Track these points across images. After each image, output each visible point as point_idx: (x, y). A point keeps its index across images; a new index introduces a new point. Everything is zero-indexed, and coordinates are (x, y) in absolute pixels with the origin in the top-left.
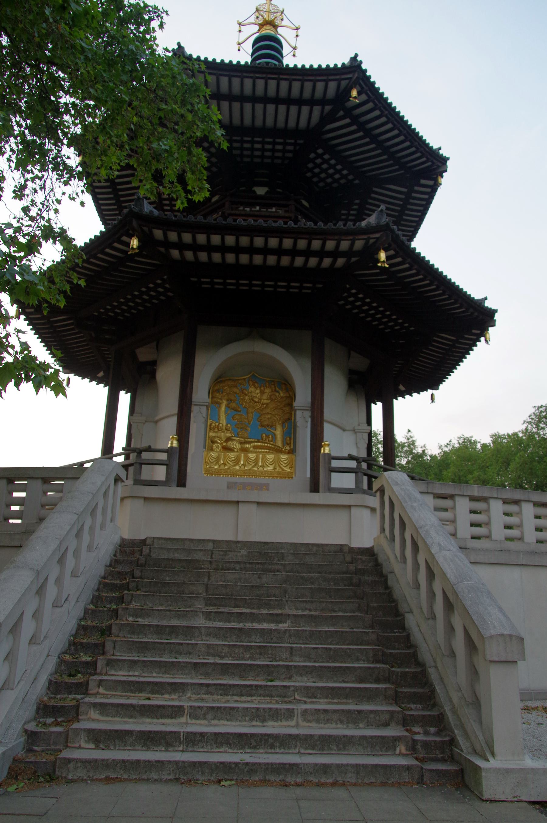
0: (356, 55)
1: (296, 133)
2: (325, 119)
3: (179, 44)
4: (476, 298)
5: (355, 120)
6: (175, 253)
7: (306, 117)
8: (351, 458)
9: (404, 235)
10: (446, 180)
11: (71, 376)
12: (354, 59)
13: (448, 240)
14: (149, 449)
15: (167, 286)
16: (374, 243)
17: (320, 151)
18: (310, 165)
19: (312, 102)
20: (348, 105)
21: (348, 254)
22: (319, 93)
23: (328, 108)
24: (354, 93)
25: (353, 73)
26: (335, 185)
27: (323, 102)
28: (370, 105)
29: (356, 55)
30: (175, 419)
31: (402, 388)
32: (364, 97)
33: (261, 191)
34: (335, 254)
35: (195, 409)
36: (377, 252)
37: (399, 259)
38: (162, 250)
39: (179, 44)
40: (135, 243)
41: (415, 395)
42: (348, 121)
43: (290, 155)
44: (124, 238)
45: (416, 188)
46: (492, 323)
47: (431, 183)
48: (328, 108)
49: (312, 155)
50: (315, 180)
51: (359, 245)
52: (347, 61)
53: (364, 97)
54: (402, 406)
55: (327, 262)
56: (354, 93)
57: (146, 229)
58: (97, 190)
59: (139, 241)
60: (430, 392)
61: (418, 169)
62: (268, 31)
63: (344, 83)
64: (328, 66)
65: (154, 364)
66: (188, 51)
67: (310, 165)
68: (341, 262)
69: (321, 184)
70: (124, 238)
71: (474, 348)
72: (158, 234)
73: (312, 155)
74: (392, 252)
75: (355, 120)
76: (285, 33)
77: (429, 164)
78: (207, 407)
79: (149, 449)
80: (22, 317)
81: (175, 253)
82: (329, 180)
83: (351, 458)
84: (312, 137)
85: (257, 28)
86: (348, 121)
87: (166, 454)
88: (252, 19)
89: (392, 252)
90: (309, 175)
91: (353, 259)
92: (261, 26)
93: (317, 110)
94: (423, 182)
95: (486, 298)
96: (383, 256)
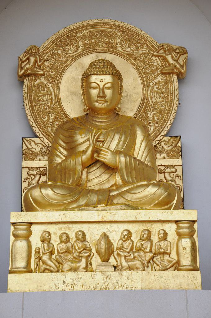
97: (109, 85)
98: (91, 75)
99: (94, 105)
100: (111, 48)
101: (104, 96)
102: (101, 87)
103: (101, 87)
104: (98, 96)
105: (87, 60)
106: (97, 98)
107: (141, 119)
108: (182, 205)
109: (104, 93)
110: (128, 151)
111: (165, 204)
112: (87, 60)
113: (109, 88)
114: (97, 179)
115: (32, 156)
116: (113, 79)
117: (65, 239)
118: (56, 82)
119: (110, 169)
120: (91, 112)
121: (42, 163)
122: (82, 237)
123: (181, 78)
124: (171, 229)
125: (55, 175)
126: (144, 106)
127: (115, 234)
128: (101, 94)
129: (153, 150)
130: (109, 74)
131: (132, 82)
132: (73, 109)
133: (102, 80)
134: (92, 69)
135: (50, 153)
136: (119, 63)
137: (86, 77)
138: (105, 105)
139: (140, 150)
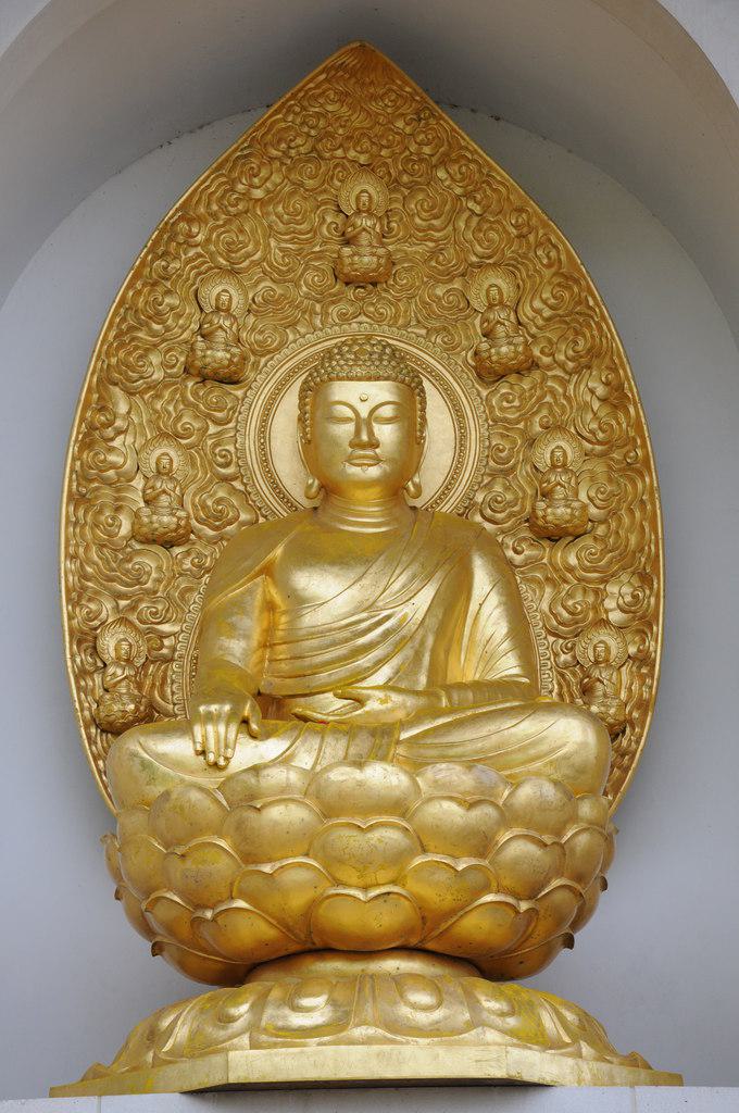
97: (387, 411)
98: (331, 380)
99: (344, 470)
101: (374, 444)
102: (364, 414)
103: (364, 414)
104: (352, 445)
106: (350, 450)
109: (371, 433)
113: (389, 421)
116: (400, 393)
128: (365, 437)
130: (386, 379)
133: (364, 397)
134: (334, 363)
138: (374, 472)
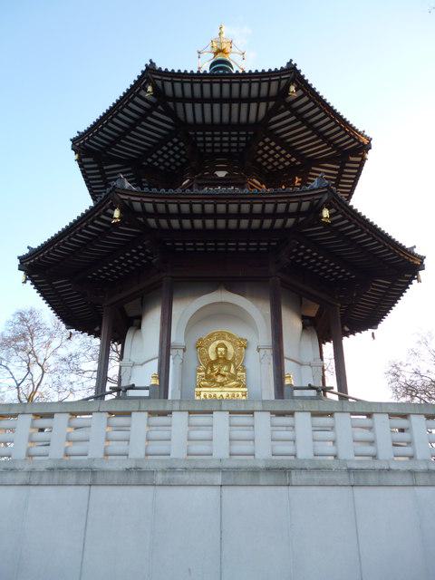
0: (291, 60)
1: (247, 126)
2: (269, 113)
3: (151, 61)
4: (407, 247)
5: (294, 111)
6: (152, 222)
7: (256, 112)
8: (311, 387)
9: (342, 192)
10: (370, 155)
11: (73, 331)
12: (290, 63)
13: (378, 198)
14: (132, 387)
15: (147, 250)
16: (318, 204)
17: (267, 140)
18: (260, 152)
19: (258, 99)
20: (289, 99)
21: (298, 213)
22: (264, 92)
23: (271, 104)
24: (292, 88)
25: (291, 73)
26: (281, 167)
27: (267, 99)
28: (306, 99)
29: (291, 60)
30: (156, 361)
31: (347, 329)
32: (300, 92)
33: (221, 174)
34: (287, 214)
35: (173, 352)
36: (320, 211)
37: (340, 216)
38: (142, 219)
39: (151, 61)
40: (117, 213)
41: (357, 334)
42: (288, 113)
43: (243, 145)
44: (109, 211)
45: (347, 165)
46: (421, 267)
47: (359, 159)
48: (271, 104)
49: (261, 144)
50: (265, 164)
51: (305, 206)
52: (284, 65)
53: (300, 92)
54: (349, 343)
55: (279, 223)
56: (292, 88)
57: (127, 202)
58: (87, 172)
59: (121, 212)
60: (370, 331)
61: (348, 150)
62: (220, 57)
63: (283, 82)
64: (270, 70)
65: (140, 318)
66: (158, 66)
67: (260, 152)
68: (290, 221)
69: (270, 167)
70: (109, 211)
71: (407, 290)
72: (137, 206)
73: (261, 144)
74: (333, 210)
75: (294, 111)
76: (231, 58)
77: (357, 143)
78: (184, 350)
79: (132, 387)
80: (29, 282)
81: (152, 222)
82: (276, 164)
83: (311, 387)
84: (260, 128)
85: (212, 55)
86: (288, 113)
87: (148, 391)
88: (209, 48)
89: (333, 210)
90: (259, 160)
91: (301, 219)
92: (216, 53)
93: (263, 105)
94: (352, 159)
95: (415, 247)
96: (326, 213)
100: (224, 339)
105: (218, 342)
107: (232, 361)
108: (244, 386)
110: (229, 371)
111: (238, 386)
112: (218, 342)
114: (219, 379)
115: (200, 371)
117: (210, 396)
118: (207, 348)
119: (224, 376)
120: (218, 358)
121: (203, 373)
122: (215, 396)
123: (245, 348)
124: (240, 393)
125: (208, 377)
126: (234, 358)
127: (225, 395)
129: (236, 370)
131: (231, 349)
132: (213, 357)
135: (206, 371)
136: (227, 343)
137: (217, 348)
139: (232, 371)
